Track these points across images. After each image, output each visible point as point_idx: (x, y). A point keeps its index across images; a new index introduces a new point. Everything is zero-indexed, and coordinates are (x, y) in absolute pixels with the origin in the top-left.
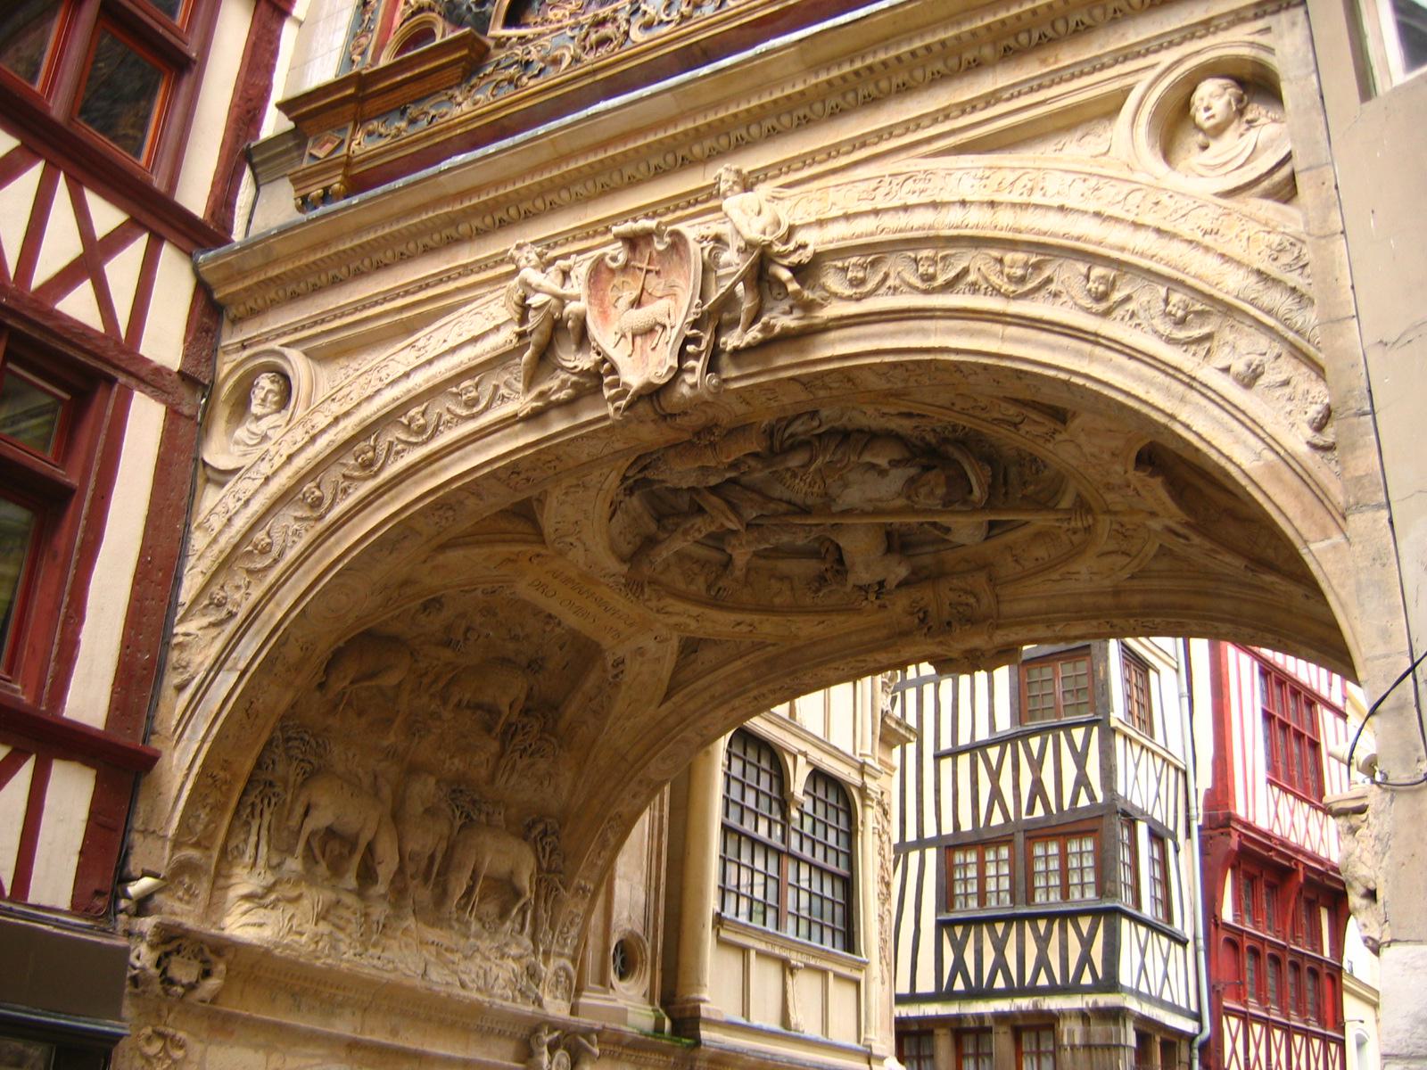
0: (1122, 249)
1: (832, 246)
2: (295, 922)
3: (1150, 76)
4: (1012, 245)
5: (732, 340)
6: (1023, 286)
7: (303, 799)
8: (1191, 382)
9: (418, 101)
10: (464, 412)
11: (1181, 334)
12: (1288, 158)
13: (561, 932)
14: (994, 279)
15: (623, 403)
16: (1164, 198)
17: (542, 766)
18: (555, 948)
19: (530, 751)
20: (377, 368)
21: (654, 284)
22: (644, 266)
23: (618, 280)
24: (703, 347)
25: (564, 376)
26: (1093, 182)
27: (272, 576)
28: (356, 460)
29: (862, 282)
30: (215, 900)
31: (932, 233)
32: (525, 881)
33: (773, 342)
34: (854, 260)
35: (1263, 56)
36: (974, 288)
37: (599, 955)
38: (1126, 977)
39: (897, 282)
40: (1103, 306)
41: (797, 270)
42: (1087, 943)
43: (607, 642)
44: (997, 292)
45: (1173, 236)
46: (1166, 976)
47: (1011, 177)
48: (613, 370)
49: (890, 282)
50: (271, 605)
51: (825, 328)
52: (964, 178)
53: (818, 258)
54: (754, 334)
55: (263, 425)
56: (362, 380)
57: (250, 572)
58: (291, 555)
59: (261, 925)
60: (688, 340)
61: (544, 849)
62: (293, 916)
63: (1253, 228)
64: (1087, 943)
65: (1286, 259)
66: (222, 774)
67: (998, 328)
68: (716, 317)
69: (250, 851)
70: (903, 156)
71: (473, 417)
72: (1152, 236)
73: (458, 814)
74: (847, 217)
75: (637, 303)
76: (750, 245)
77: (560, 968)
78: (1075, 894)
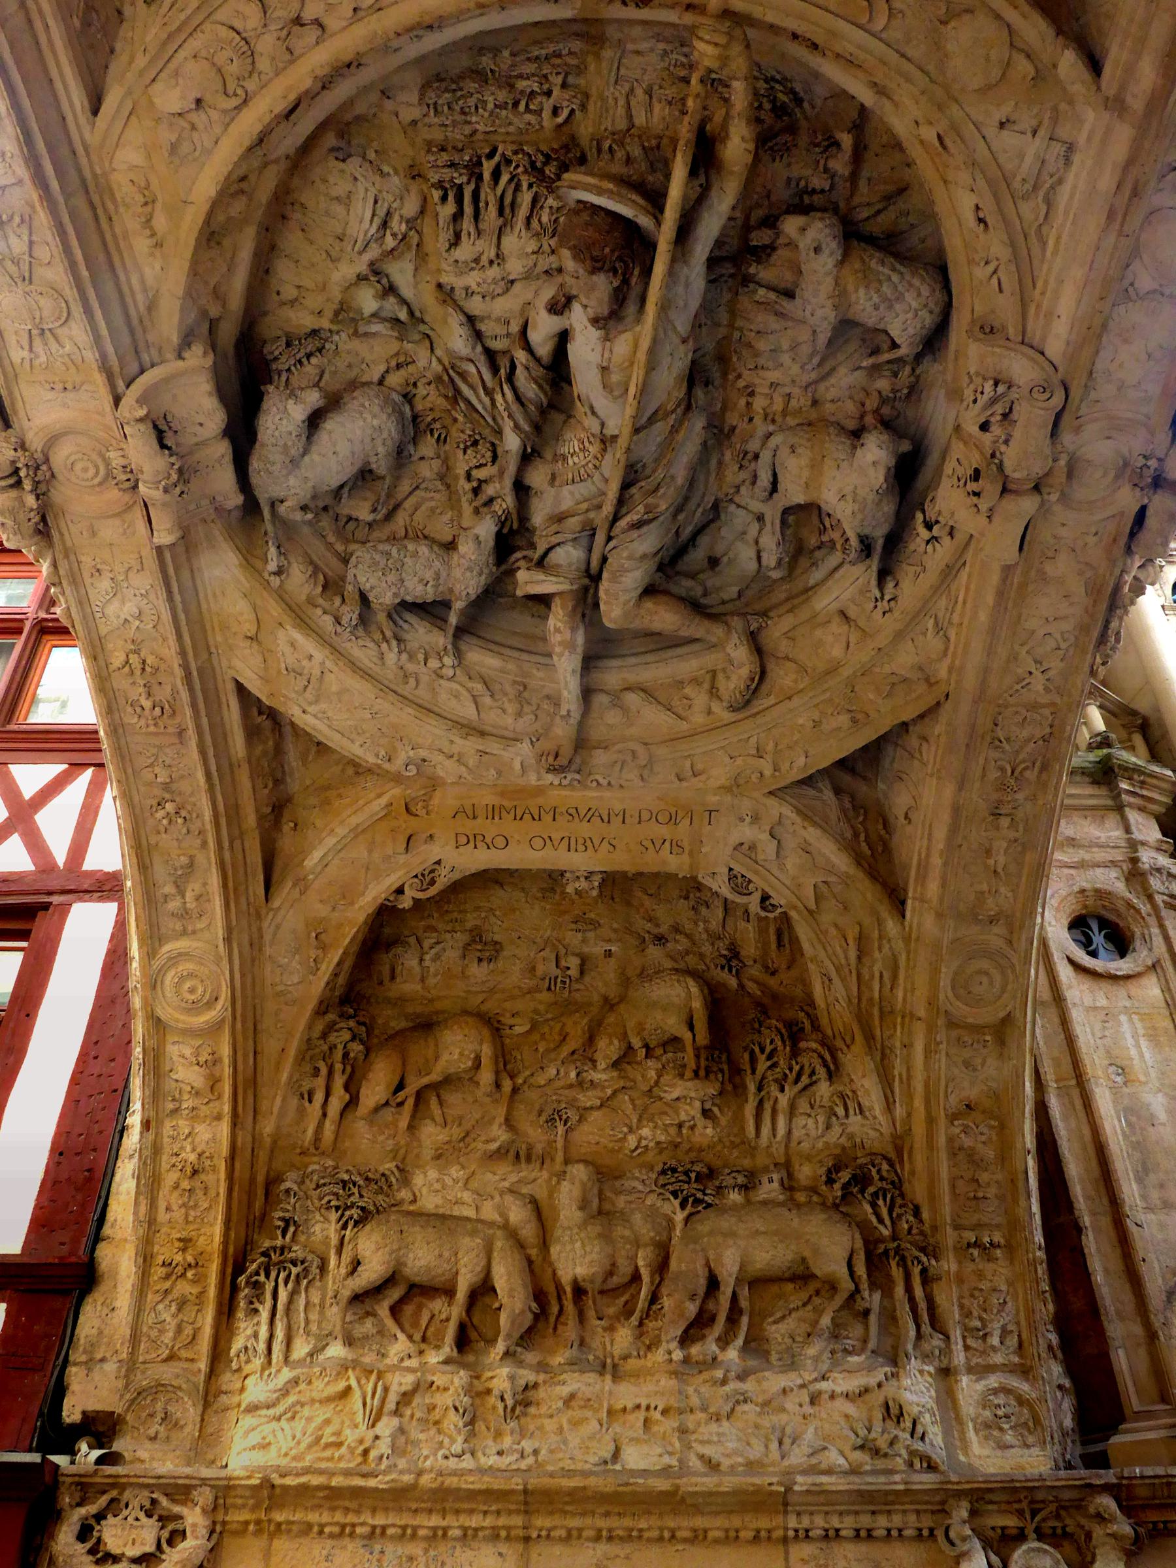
2: (329, 1430)
7: (346, 1257)
13: (967, 1331)
17: (824, 1089)
18: (959, 1357)
19: (792, 1077)
30: (210, 1430)
37: (1142, 1352)
43: (675, 863)
59: (264, 1446)
61: (874, 1205)
62: (327, 1422)
66: (179, 1258)
69: (262, 1346)
73: (677, 1203)
77: (995, 1391)
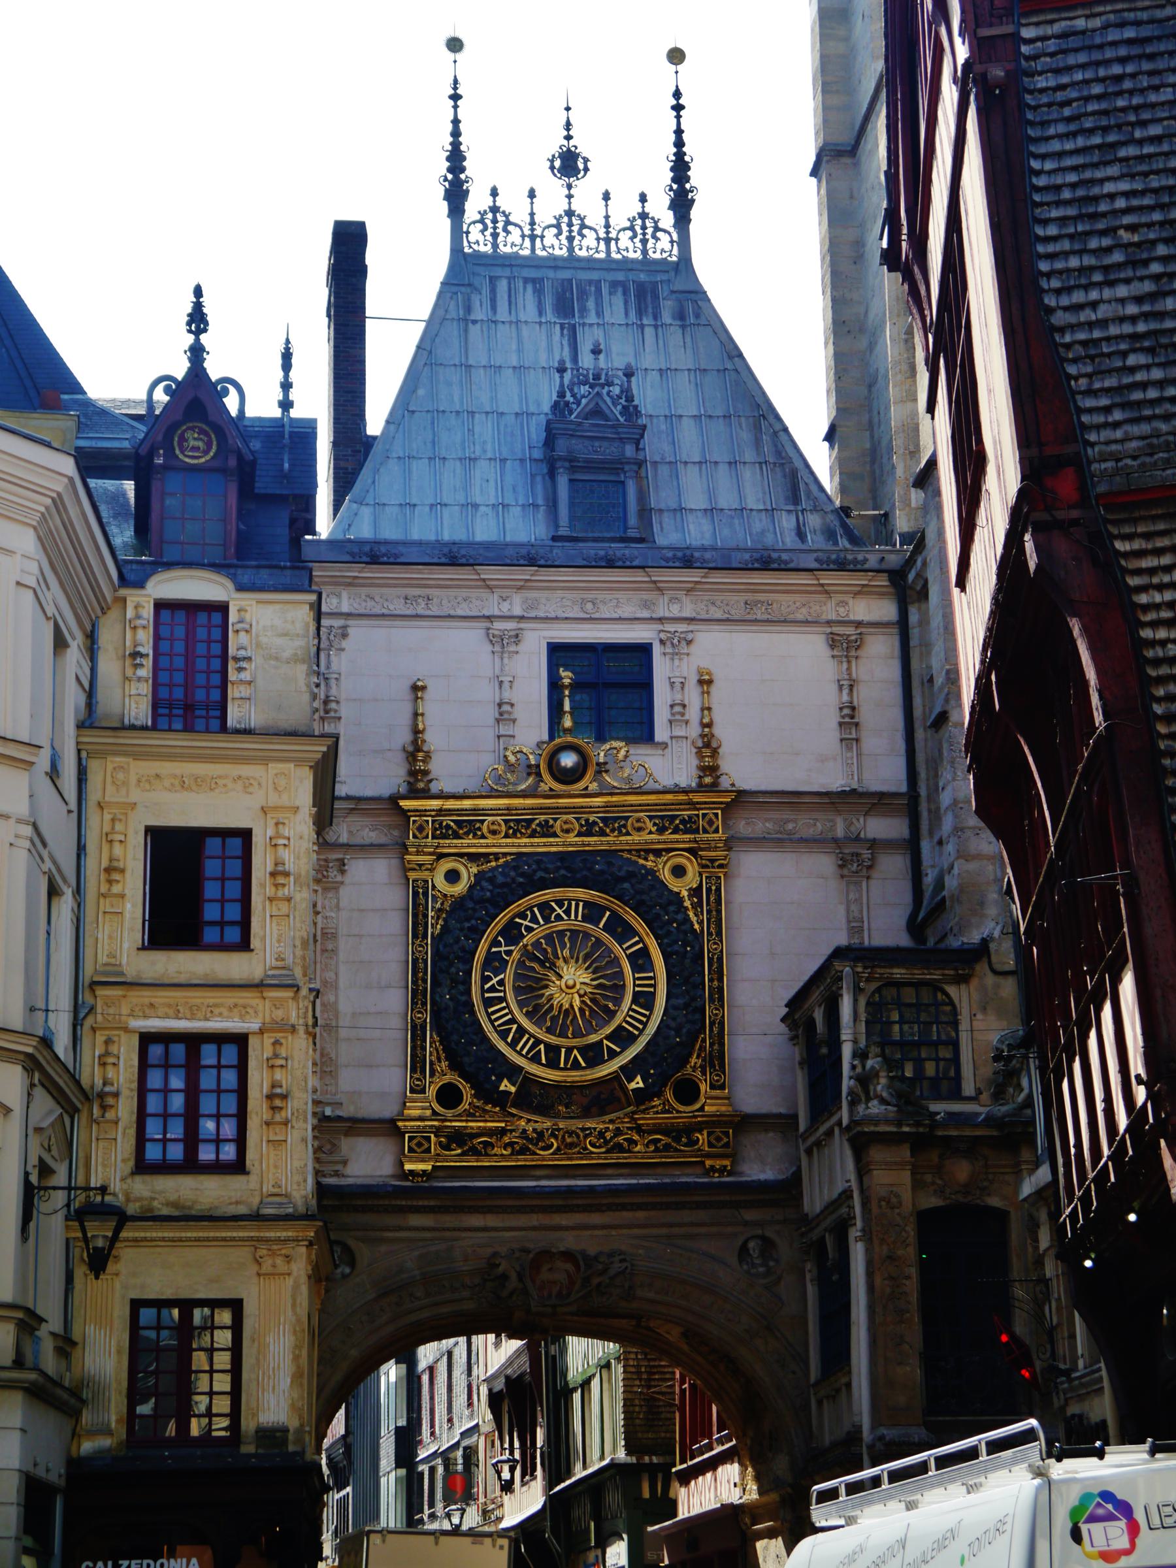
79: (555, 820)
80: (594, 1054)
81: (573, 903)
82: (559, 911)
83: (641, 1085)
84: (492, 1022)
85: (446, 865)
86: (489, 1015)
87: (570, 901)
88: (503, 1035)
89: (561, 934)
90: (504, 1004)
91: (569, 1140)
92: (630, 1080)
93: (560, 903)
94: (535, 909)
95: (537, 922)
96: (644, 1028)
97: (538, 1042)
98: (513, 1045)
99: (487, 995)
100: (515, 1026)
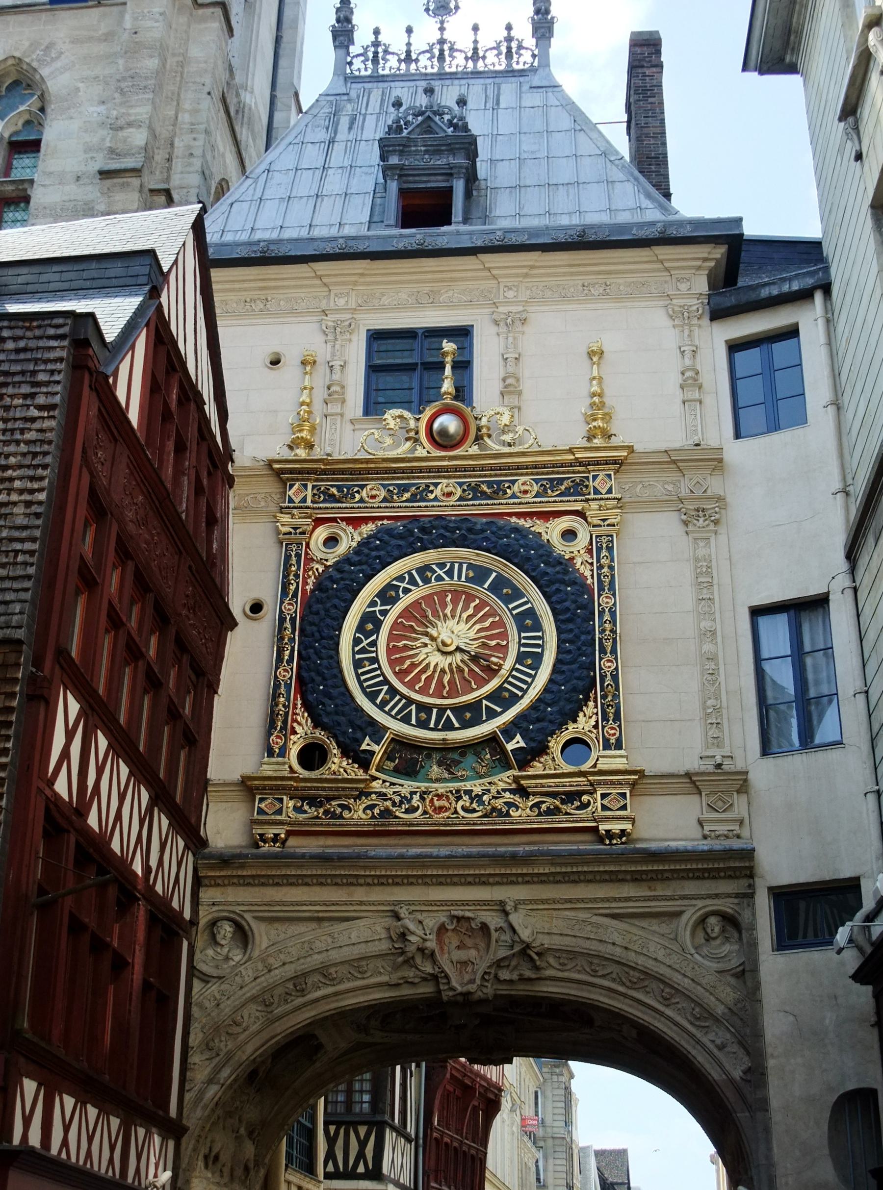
0: (679, 985)
1: (555, 947)
3: (692, 910)
4: (634, 969)
5: (504, 975)
6: (633, 986)
8: (698, 1042)
9: (329, 799)
10: (359, 976)
11: (697, 1023)
12: (743, 963)
14: (624, 979)
15: (451, 993)
16: (696, 967)
20: (309, 942)
21: (469, 942)
22: (463, 930)
23: (449, 934)
24: (492, 976)
25: (418, 973)
26: (668, 951)
27: (242, 1037)
28: (295, 987)
29: (565, 965)
31: (601, 954)
32: (251, 1165)
33: (523, 979)
34: (564, 955)
35: (736, 915)
36: (614, 980)
38: (385, 1171)
39: (581, 969)
40: (666, 1003)
41: (539, 954)
42: (363, 1144)
44: (623, 984)
45: (699, 984)
46: (402, 1166)
47: (635, 938)
48: (447, 977)
49: (578, 968)
50: (239, 1053)
51: (546, 979)
52: (615, 931)
53: (549, 949)
54: (515, 977)
55: (226, 950)
56: (298, 946)
57: (227, 1033)
58: (254, 1028)
60: (485, 973)
63: (729, 990)
64: (363, 1144)
65: (739, 1005)
67: (622, 998)
68: (499, 964)
70: (586, 911)
71: (364, 978)
72: (690, 982)
74: (561, 934)
75: (458, 947)
76: (523, 942)
78: (357, 1109)
79: (436, 485)
80: (471, 714)
81: (456, 565)
82: (440, 572)
83: (522, 744)
84: (360, 683)
85: (321, 533)
86: (358, 676)
87: (452, 564)
88: (372, 697)
89: (442, 594)
90: (376, 666)
91: (437, 803)
92: (510, 738)
93: (441, 566)
94: (414, 572)
95: (416, 584)
96: (528, 689)
97: (410, 701)
98: (381, 707)
99: (357, 656)
100: (386, 688)
